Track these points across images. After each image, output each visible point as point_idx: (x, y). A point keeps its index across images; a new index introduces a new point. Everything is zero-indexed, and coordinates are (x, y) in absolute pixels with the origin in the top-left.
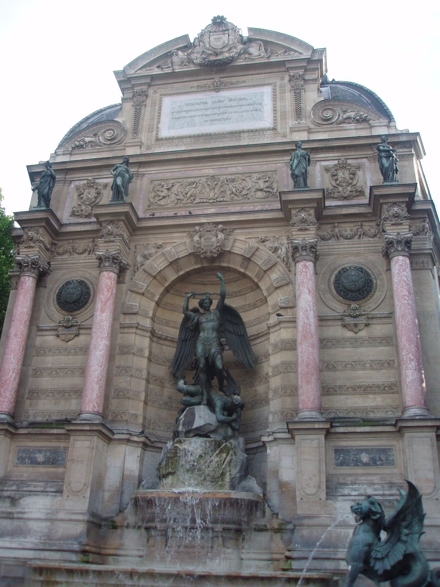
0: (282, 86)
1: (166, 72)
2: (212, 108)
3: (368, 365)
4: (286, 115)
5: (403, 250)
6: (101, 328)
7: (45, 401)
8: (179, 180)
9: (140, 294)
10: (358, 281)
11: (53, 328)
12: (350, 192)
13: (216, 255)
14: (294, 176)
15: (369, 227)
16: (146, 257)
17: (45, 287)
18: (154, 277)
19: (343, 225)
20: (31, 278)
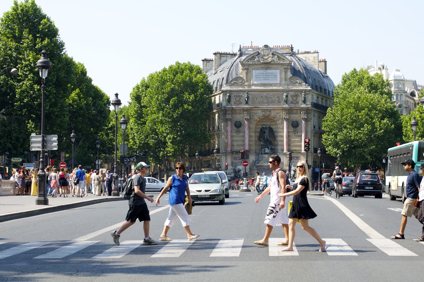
14: (285, 101)
16: (253, 116)
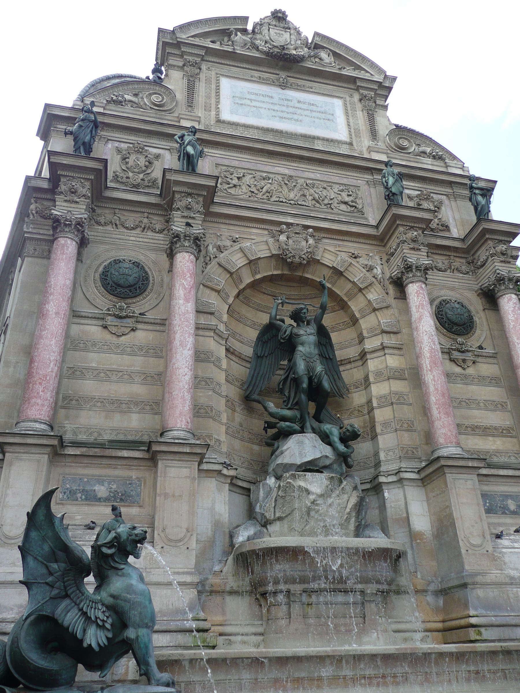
0: (352, 104)
1: (226, 49)
2: (279, 105)
3: (482, 404)
4: (360, 133)
5: (513, 288)
6: (187, 321)
7: (91, 413)
8: (250, 172)
9: (216, 291)
10: (463, 315)
11: (98, 316)
12: (438, 224)
13: (305, 262)
15: (458, 263)
16: (220, 249)
17: (82, 262)
18: (231, 274)
19: (436, 257)
20: (74, 243)
